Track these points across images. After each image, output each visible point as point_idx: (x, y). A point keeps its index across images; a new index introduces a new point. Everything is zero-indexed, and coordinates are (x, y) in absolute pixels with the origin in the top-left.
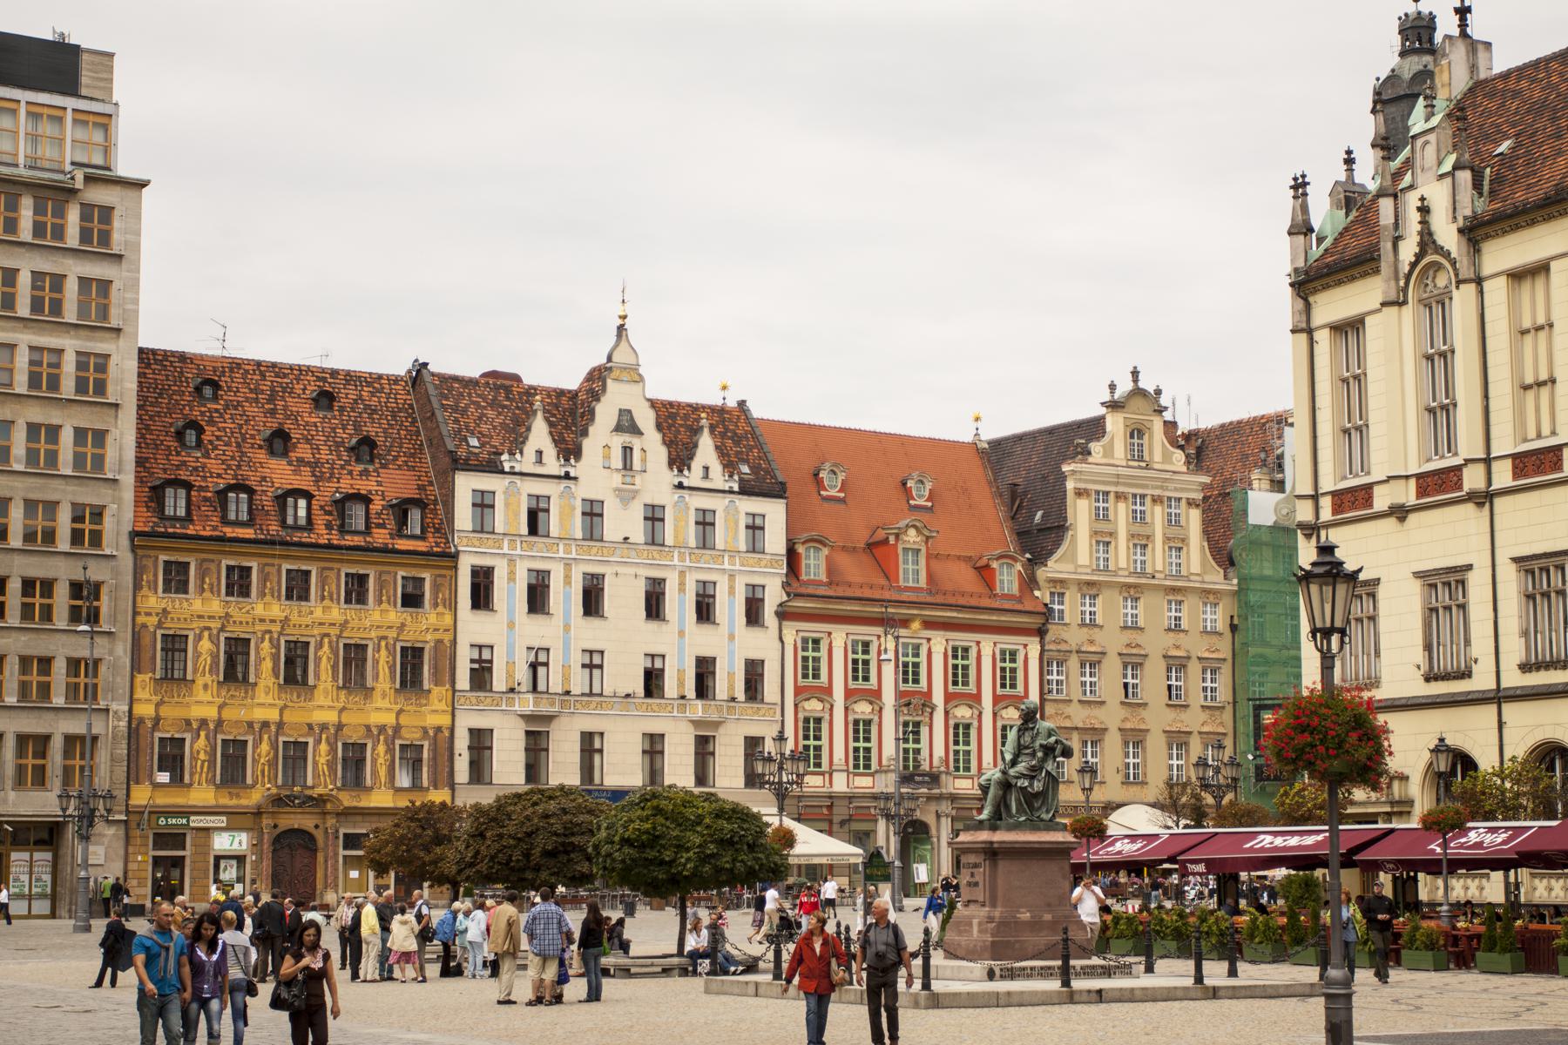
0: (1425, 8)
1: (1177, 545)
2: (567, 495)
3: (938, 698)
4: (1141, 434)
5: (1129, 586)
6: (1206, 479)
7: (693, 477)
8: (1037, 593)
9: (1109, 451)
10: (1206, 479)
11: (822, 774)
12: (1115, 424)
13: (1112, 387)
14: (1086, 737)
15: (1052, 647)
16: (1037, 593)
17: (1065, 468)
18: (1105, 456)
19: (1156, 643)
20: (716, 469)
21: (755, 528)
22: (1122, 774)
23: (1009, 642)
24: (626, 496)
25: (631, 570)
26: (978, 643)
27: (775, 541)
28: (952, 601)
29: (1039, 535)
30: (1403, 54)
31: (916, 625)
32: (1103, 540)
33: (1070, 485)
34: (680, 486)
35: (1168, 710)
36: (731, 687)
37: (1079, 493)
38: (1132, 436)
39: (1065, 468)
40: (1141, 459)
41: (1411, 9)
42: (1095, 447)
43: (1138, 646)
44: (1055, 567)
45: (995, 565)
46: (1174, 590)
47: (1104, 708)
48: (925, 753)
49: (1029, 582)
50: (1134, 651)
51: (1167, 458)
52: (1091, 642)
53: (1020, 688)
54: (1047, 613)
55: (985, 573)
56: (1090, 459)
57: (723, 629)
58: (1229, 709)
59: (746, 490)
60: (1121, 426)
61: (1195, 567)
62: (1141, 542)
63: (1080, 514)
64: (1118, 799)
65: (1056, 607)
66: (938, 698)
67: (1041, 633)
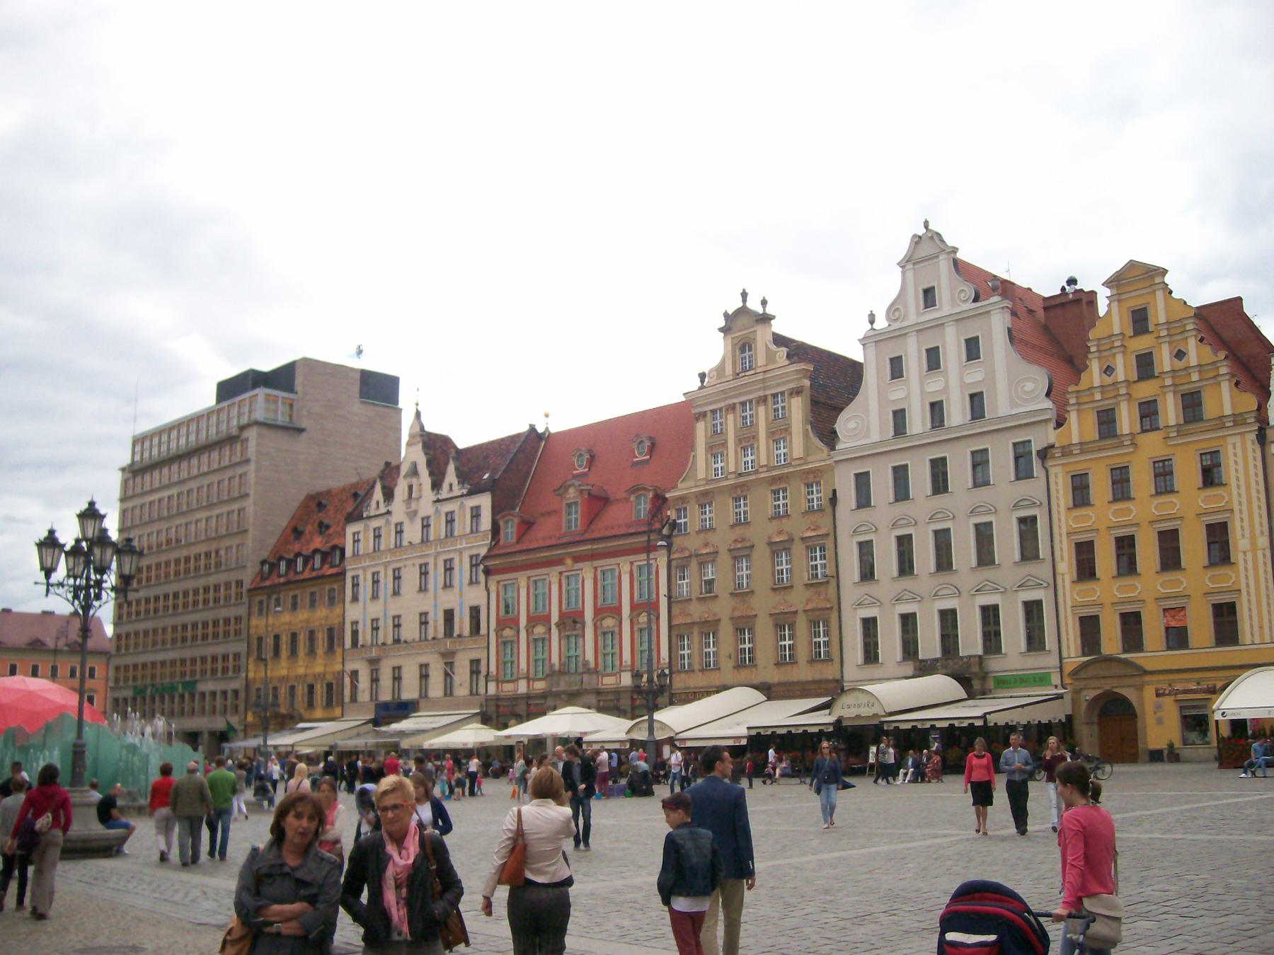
1: (779, 433)
2: (388, 522)
7: (444, 494)
18: (718, 378)
19: (761, 532)
20: (455, 482)
21: (476, 513)
24: (412, 515)
25: (411, 562)
27: (486, 523)
34: (438, 501)
36: (461, 628)
43: (744, 540)
51: (770, 357)
52: (706, 545)
57: (456, 589)
59: (471, 493)
64: (729, 682)
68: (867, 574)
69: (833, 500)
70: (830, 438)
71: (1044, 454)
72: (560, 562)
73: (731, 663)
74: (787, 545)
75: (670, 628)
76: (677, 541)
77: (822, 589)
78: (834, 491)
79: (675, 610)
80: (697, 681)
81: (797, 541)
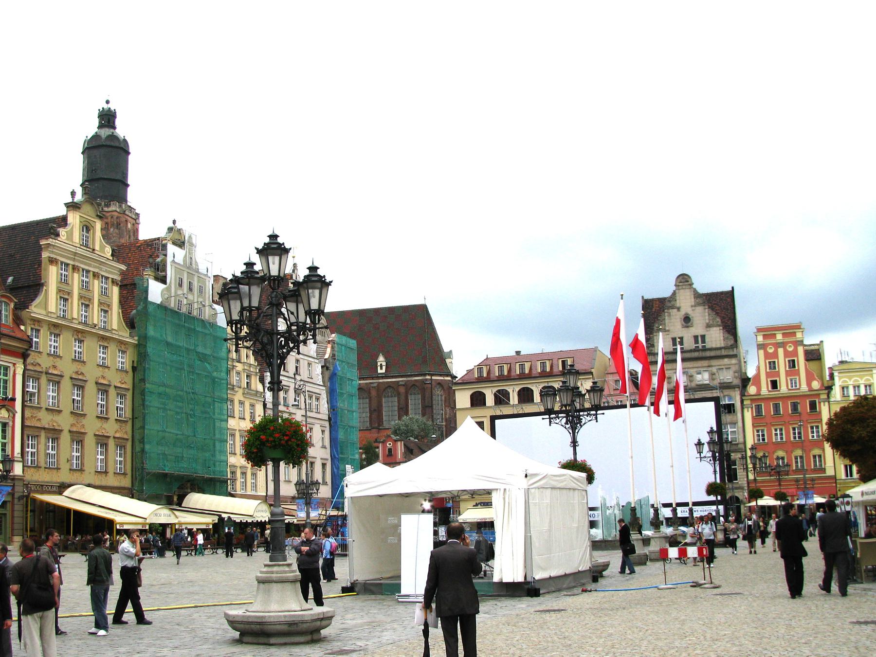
0: (112, 106)
5: (78, 331)
6: (123, 267)
9: (70, 235)
10: (123, 267)
12: (74, 219)
13: (73, 194)
30: (101, 126)
32: (64, 297)
33: (45, 255)
37: (52, 261)
39: (43, 242)
41: (106, 106)
42: (62, 232)
44: (35, 310)
46: (104, 338)
49: (18, 320)
51: (102, 248)
61: (115, 326)
62: (86, 303)
63: (52, 275)
67: (24, 356)
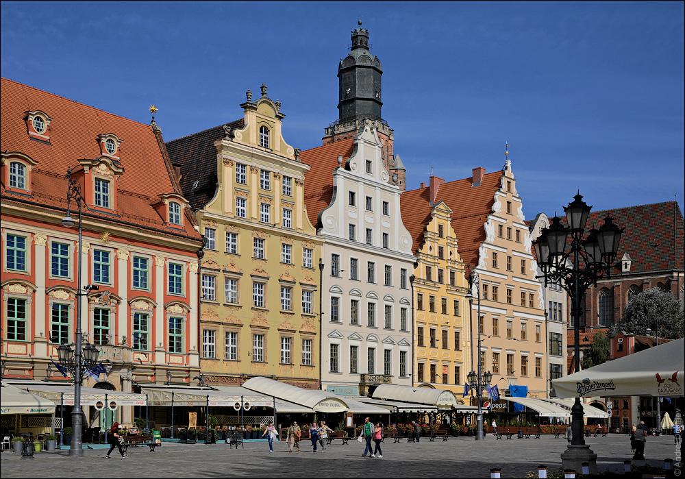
3: (123, 293)
4: (267, 131)
8: (196, 227)
11: (26, 344)
14: (228, 330)
15: (206, 265)
16: (196, 227)
17: (217, 144)
18: (243, 140)
19: (274, 270)
22: (252, 355)
23: (177, 258)
26: (154, 256)
28: (133, 221)
29: (201, 188)
31: (106, 235)
35: (282, 315)
37: (227, 162)
38: (261, 131)
39: (217, 144)
40: (266, 146)
44: (210, 209)
45: (167, 202)
47: (240, 310)
48: (112, 332)
49: (190, 220)
50: (261, 275)
51: (283, 149)
53: (184, 292)
54: (203, 241)
55: (158, 206)
56: (234, 140)
58: (317, 318)
60: (255, 122)
63: (227, 176)
65: (209, 239)
66: (123, 293)
67: (200, 255)
68: (335, 318)
69: (321, 266)
70: (319, 226)
71: (412, 279)
72: (98, 232)
73: (250, 358)
74: (291, 285)
75: (199, 321)
76: (208, 255)
77: (311, 319)
78: (320, 259)
79: (204, 307)
80: (223, 368)
81: (298, 284)
